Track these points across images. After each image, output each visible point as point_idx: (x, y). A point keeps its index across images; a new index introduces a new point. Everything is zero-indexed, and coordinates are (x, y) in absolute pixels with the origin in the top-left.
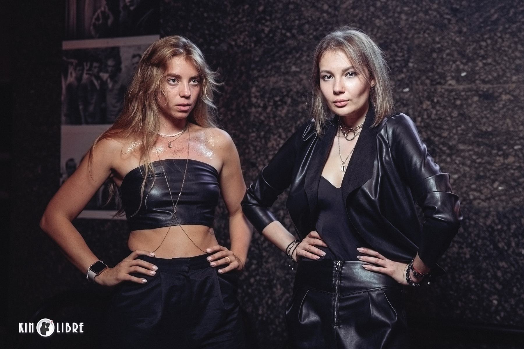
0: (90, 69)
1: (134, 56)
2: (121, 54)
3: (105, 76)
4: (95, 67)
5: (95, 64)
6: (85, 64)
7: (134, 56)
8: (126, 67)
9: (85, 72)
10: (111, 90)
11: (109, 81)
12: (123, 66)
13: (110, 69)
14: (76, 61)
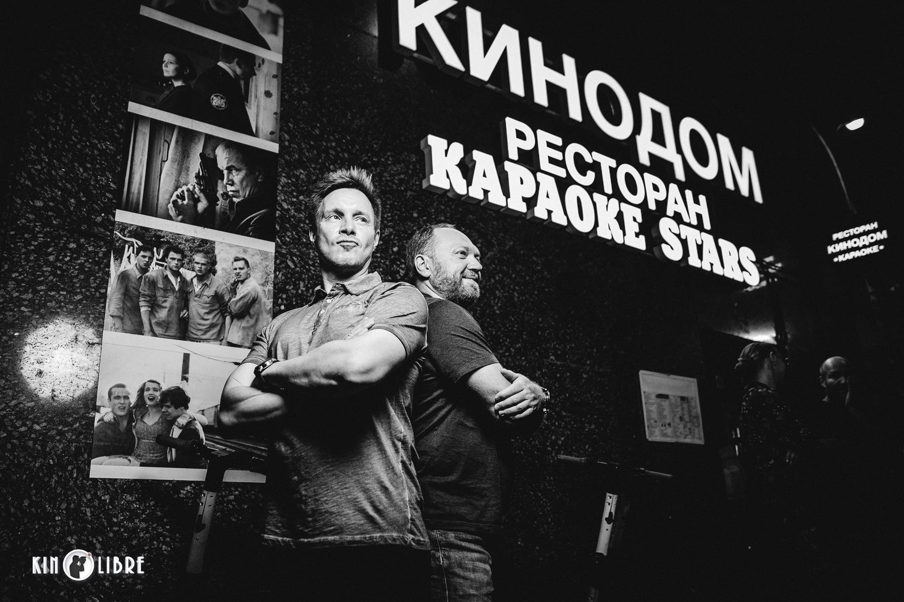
0: (163, 260)
1: (237, 259)
2: (216, 252)
3: (189, 275)
4: (173, 259)
5: (172, 254)
6: (155, 249)
7: (237, 259)
8: (223, 269)
9: (155, 261)
10: (199, 296)
11: (195, 281)
12: (218, 267)
13: (197, 267)
14: (140, 244)
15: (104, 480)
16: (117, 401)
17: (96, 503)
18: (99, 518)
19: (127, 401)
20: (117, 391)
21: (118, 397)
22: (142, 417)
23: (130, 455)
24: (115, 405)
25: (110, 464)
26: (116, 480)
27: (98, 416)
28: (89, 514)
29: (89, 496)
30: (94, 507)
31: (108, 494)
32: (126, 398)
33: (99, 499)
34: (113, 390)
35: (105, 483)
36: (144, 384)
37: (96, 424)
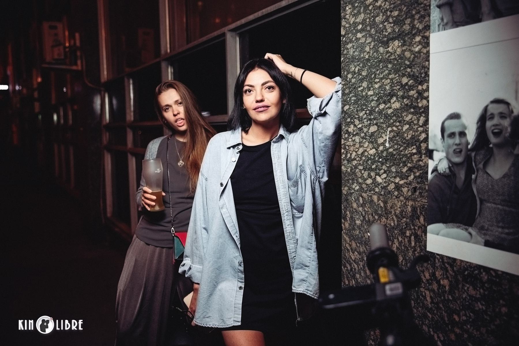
15: (442, 256)
16: (451, 141)
17: (435, 286)
18: (438, 308)
19: (463, 140)
20: (453, 126)
21: (452, 135)
22: (485, 165)
23: (471, 225)
24: (449, 147)
25: (447, 236)
26: (454, 260)
27: (431, 165)
28: (428, 299)
29: (427, 275)
30: (433, 291)
31: (447, 278)
32: (462, 134)
33: (438, 282)
34: (446, 124)
35: (443, 262)
36: (486, 109)
37: (430, 176)
